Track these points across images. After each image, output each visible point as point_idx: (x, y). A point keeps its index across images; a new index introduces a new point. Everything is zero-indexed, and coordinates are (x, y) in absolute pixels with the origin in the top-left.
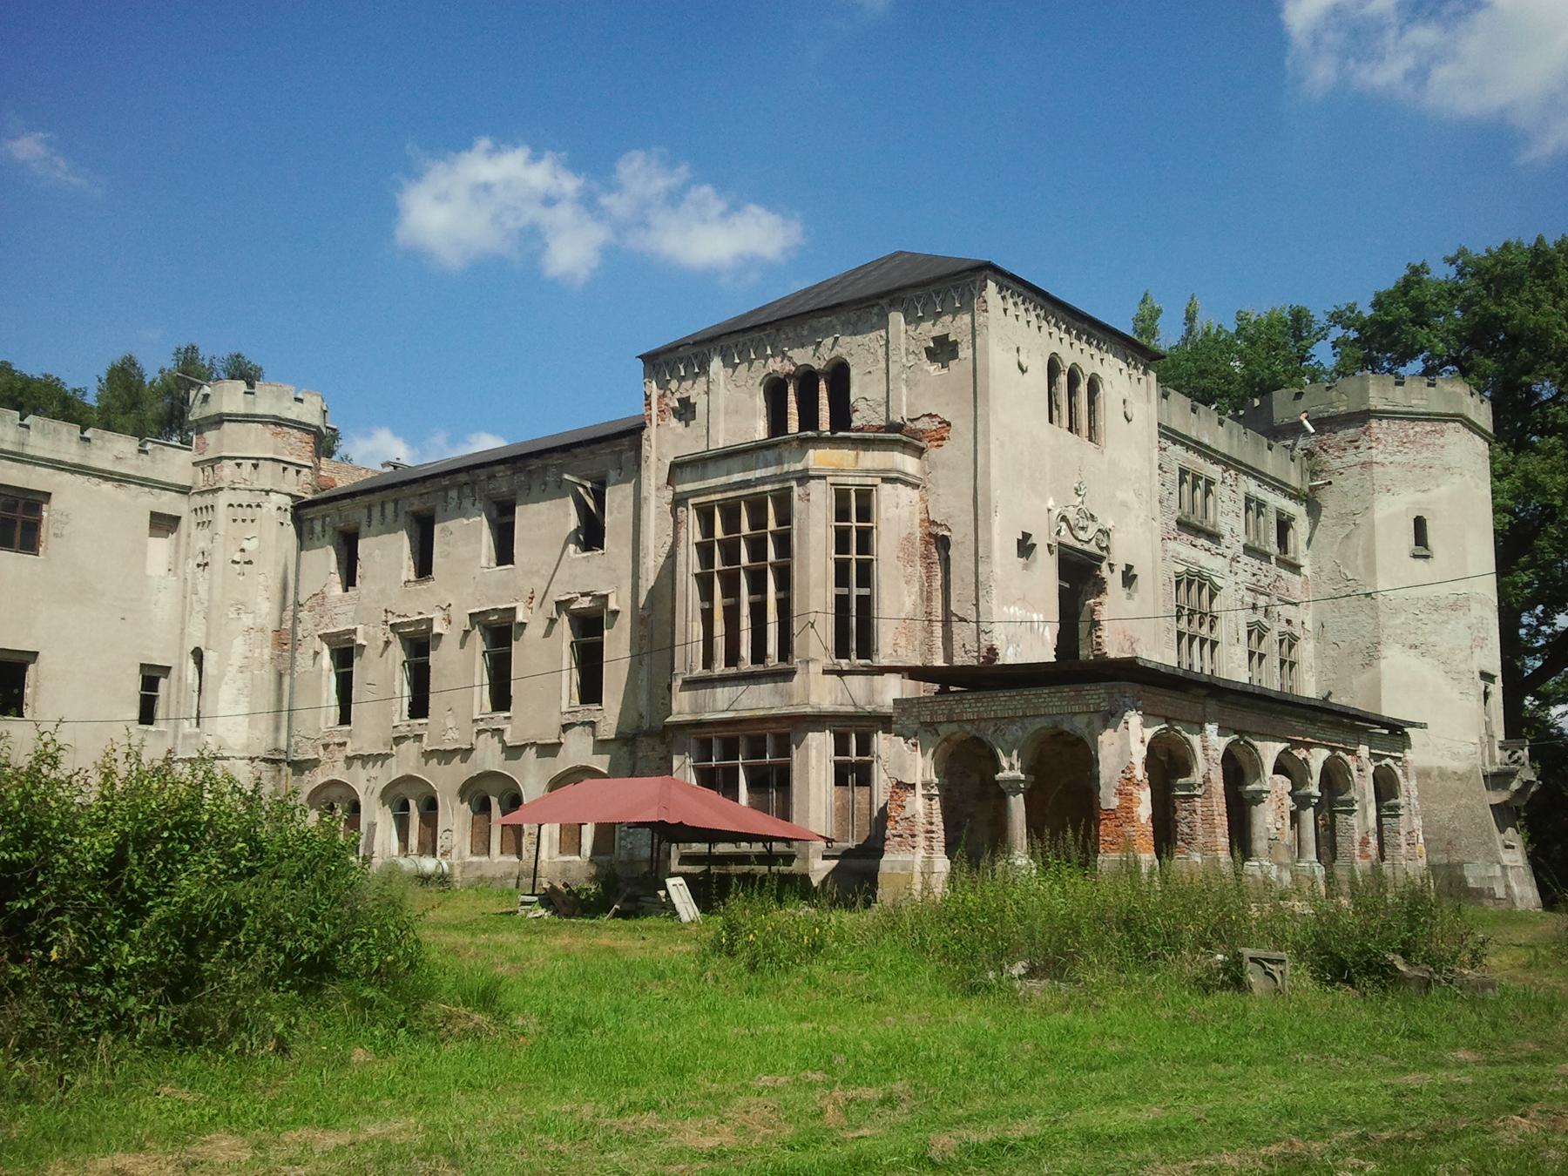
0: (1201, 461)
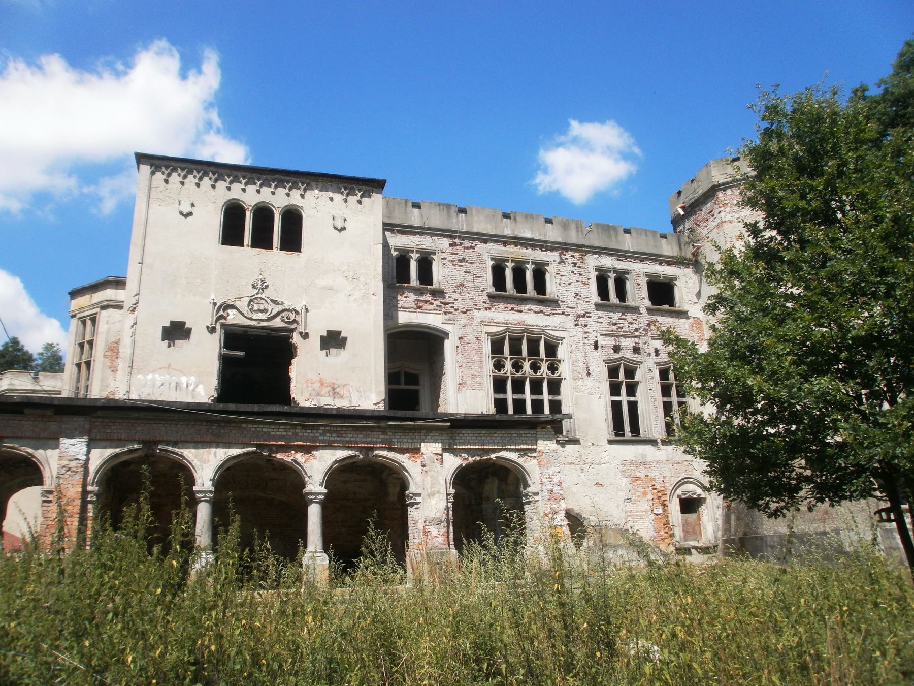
0: (530, 251)
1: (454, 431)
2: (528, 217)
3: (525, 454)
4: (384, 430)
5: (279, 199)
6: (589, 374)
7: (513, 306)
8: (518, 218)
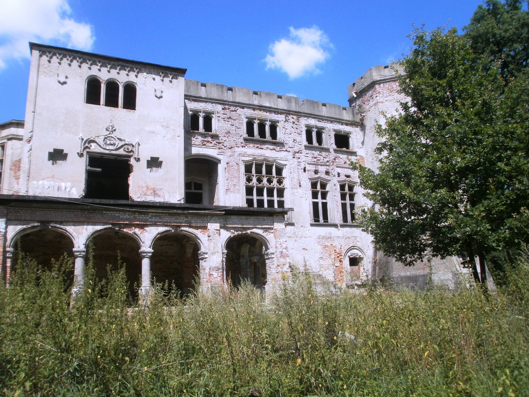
0: (268, 114)
1: (226, 216)
2: (268, 94)
3: (267, 231)
4: (186, 215)
5: (122, 77)
6: (300, 186)
7: (258, 145)
8: (262, 95)
